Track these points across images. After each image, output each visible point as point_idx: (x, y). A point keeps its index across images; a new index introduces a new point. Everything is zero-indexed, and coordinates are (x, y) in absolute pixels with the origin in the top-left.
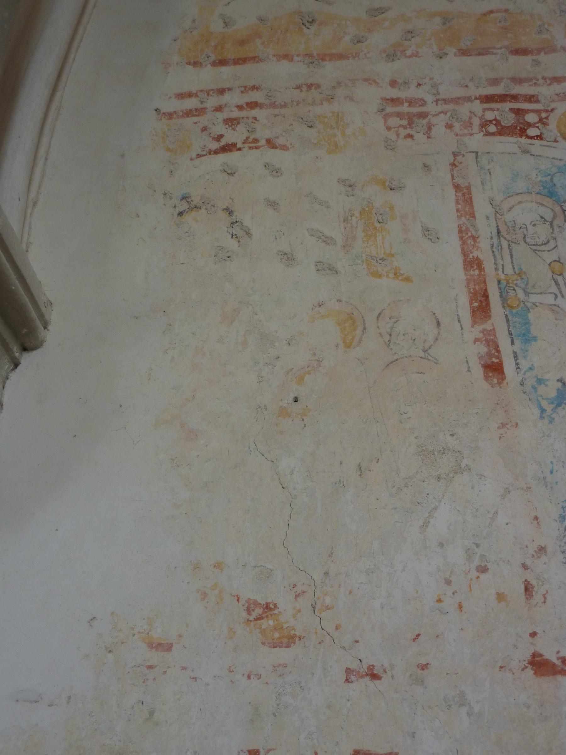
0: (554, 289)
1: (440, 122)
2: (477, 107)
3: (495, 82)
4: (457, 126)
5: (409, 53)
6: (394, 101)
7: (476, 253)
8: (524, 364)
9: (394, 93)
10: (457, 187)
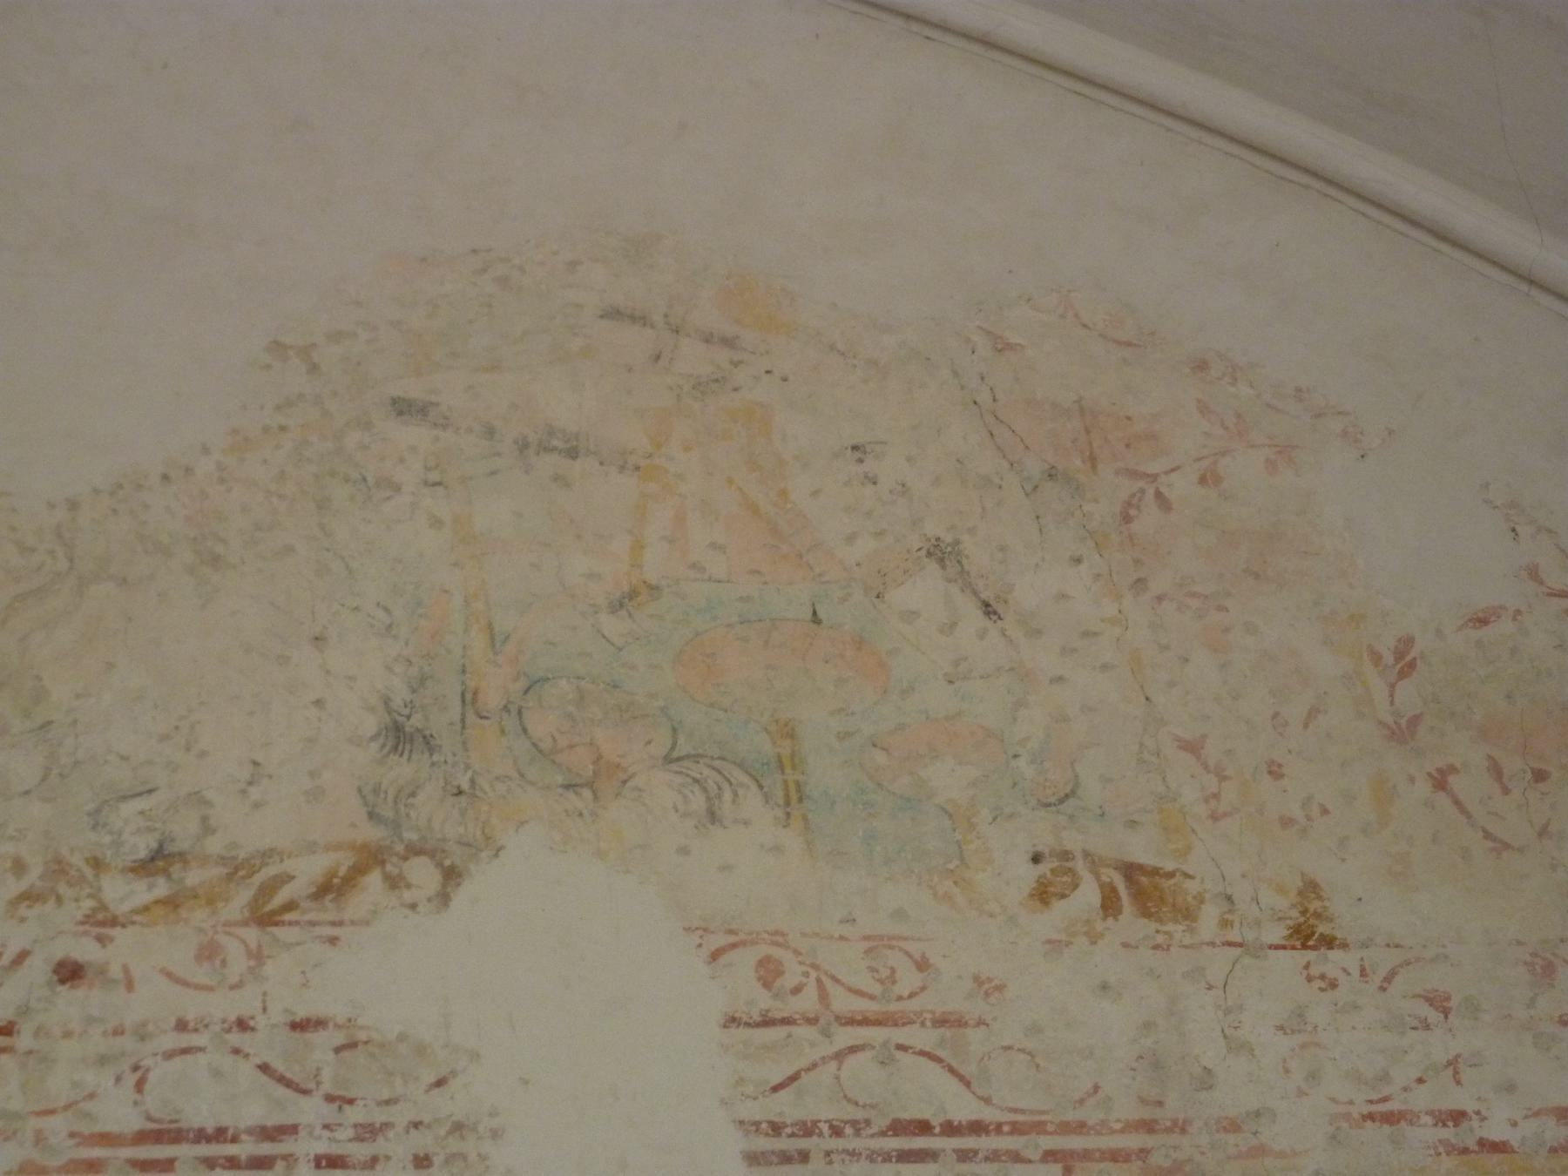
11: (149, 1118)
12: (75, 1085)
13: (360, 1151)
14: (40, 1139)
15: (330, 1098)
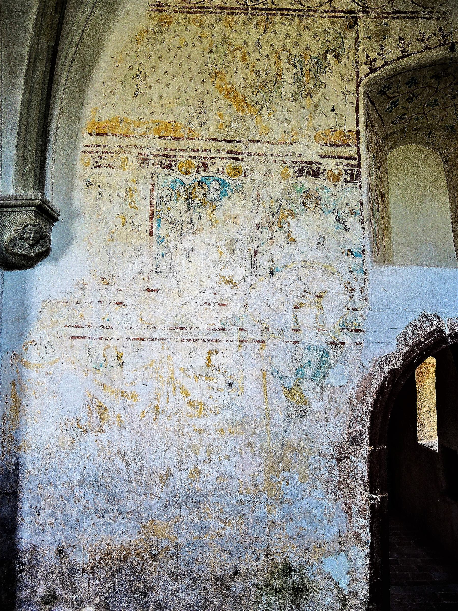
0: (167, 214)
1: (151, 162)
2: (160, 158)
3: (166, 150)
4: (155, 164)
5: (146, 137)
6: (141, 154)
7: (153, 203)
8: (157, 232)
9: (141, 151)
10: (151, 184)
11: (394, 9)
12: (382, 3)
13: (428, 16)
14: (377, 12)
15: (423, 7)
